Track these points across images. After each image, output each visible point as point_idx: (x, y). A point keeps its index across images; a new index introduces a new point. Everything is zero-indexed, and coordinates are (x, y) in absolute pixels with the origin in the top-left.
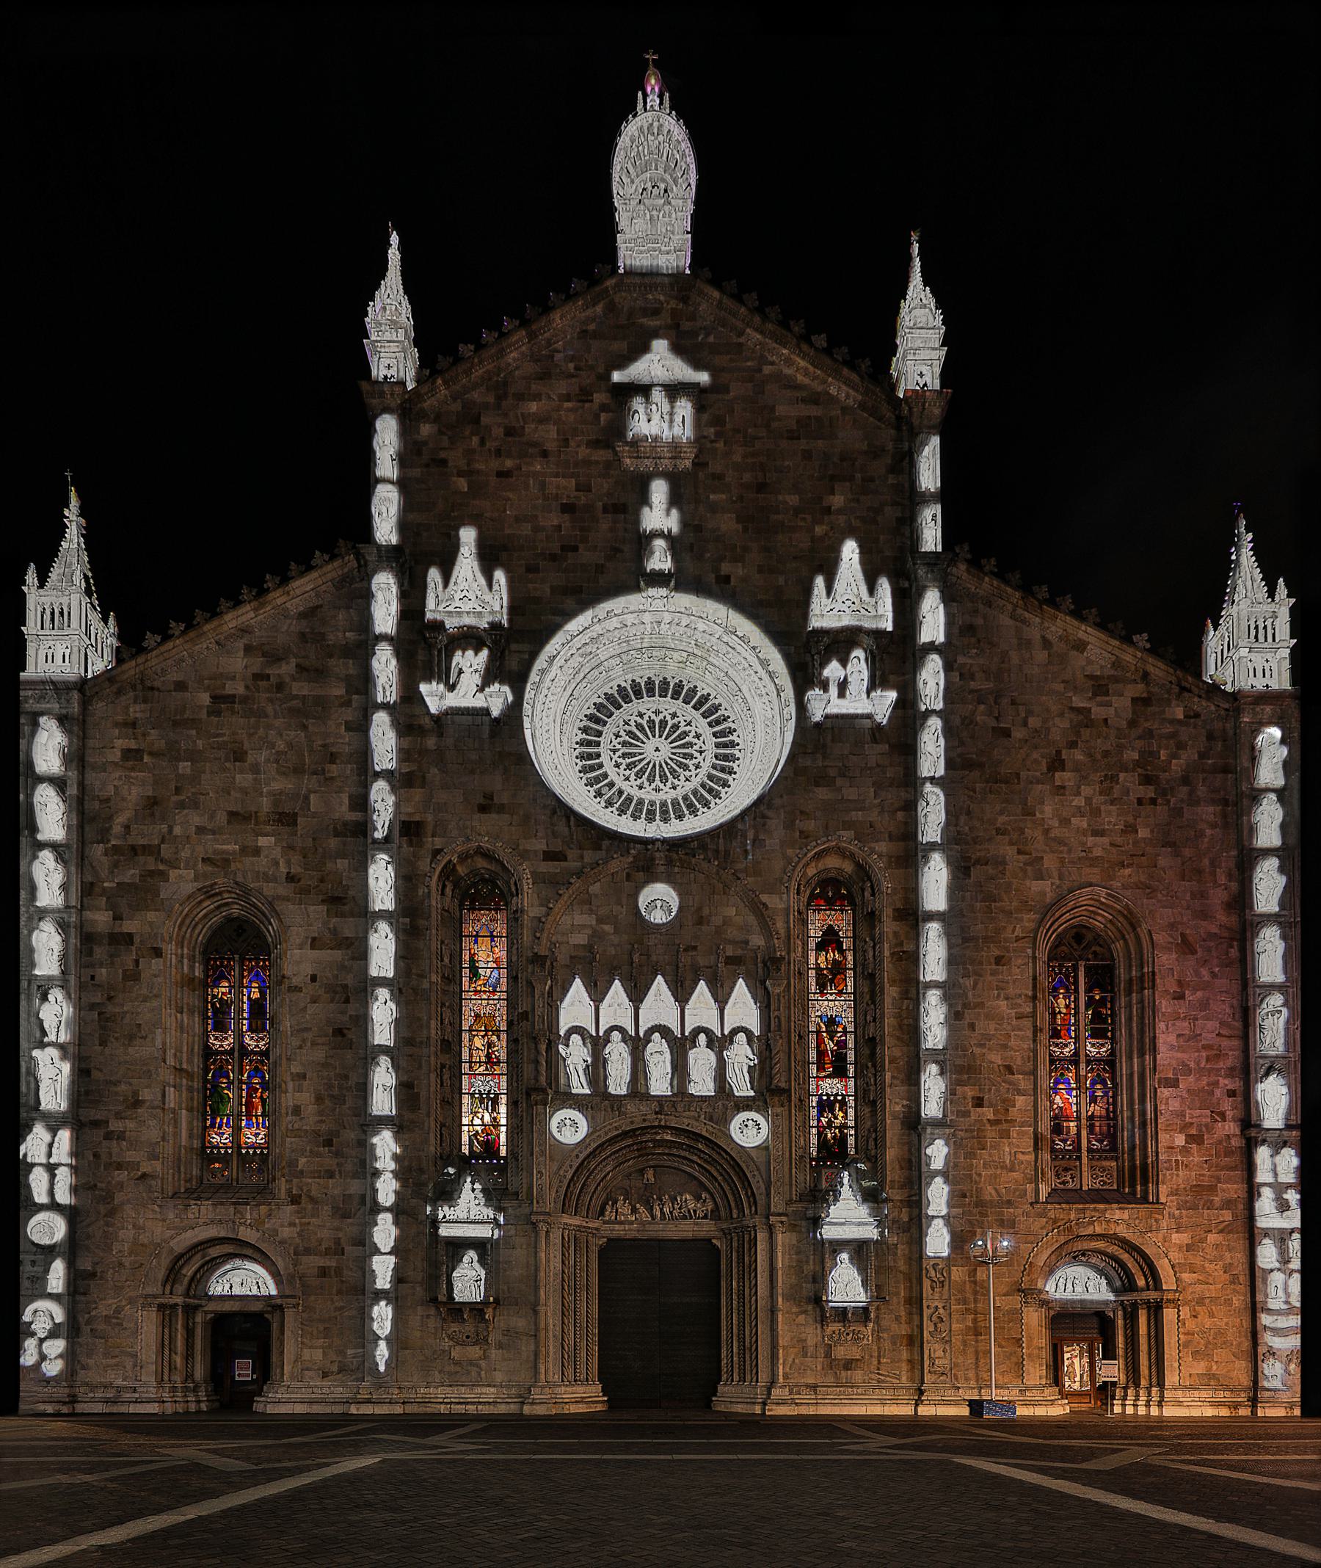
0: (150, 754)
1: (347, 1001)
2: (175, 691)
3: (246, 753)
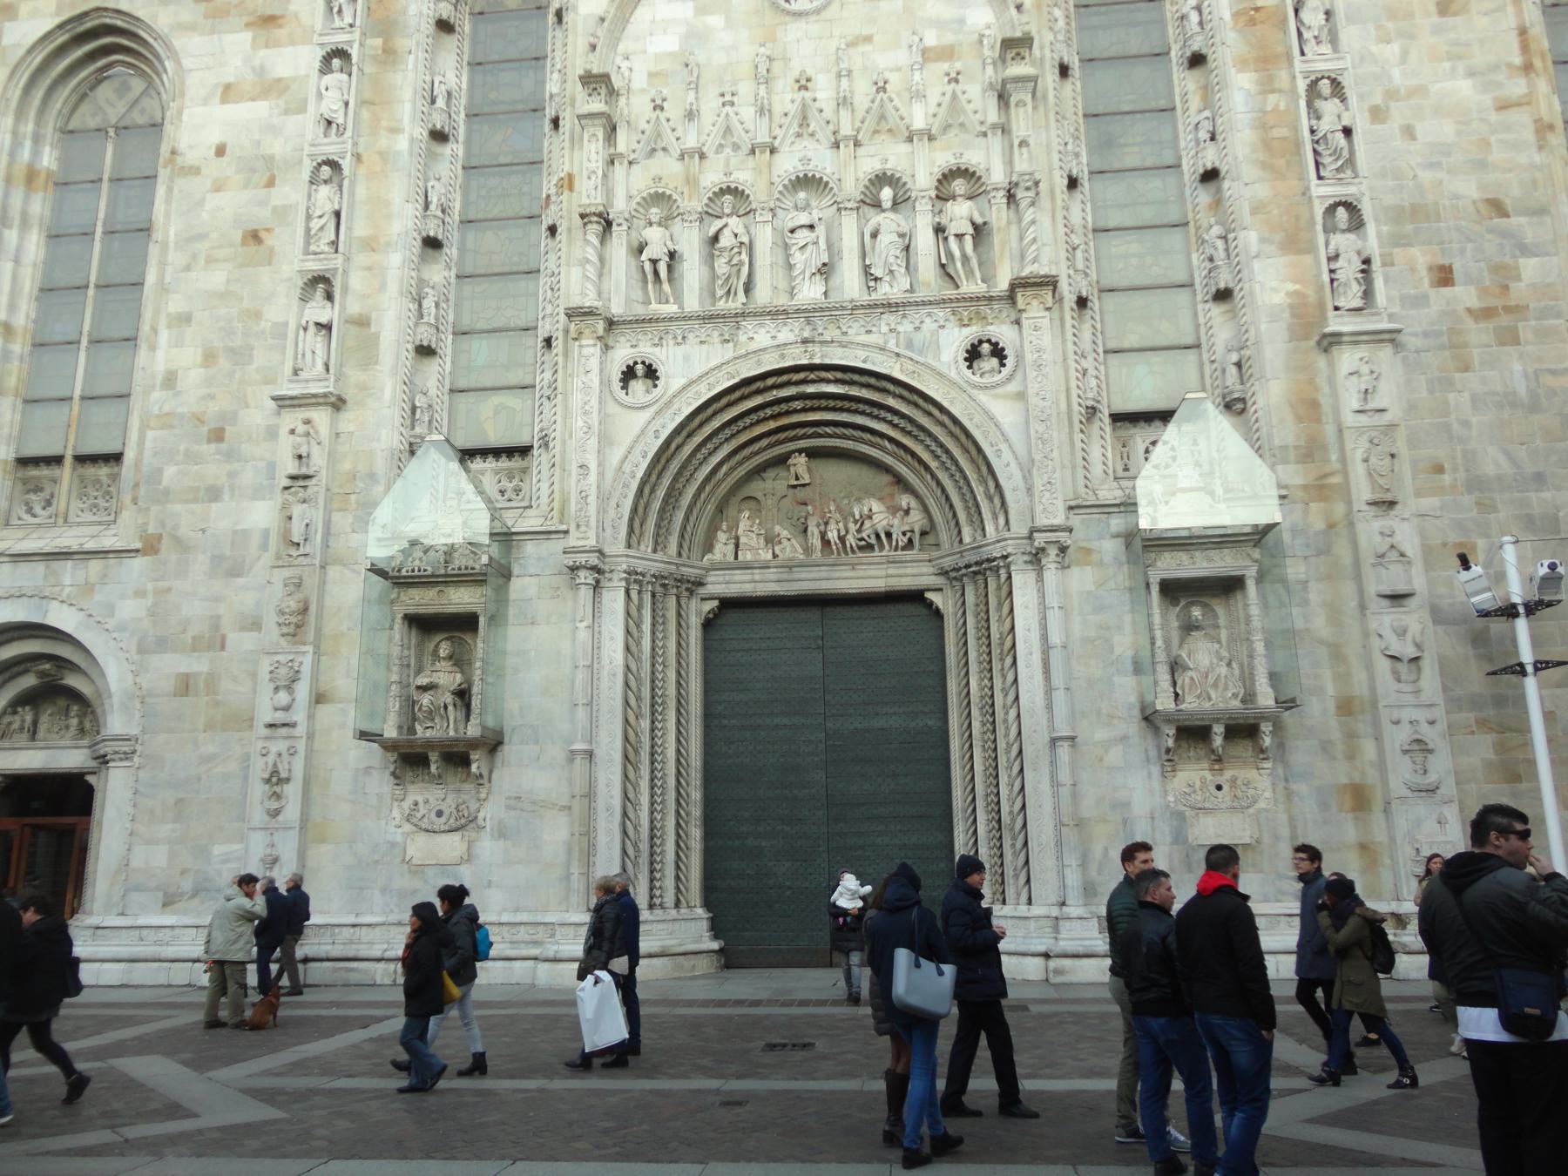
1: (271, 183)
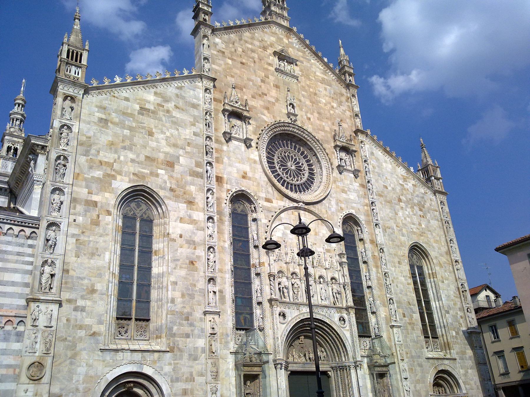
0: (112, 123)
1: (195, 249)
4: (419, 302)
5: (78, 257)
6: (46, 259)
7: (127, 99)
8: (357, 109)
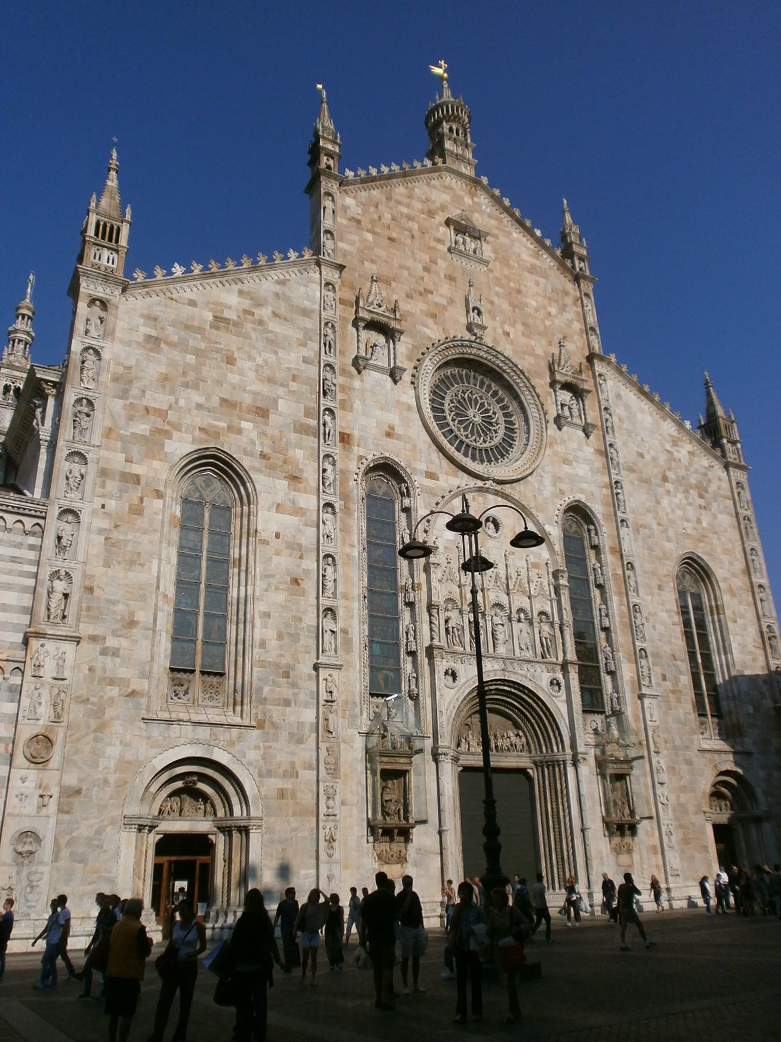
0: (166, 343)
1: (301, 557)
2: (188, 305)
3: (235, 359)
4: (692, 656)
5: (109, 567)
6: (57, 569)
7: (192, 303)
8: (592, 319)
